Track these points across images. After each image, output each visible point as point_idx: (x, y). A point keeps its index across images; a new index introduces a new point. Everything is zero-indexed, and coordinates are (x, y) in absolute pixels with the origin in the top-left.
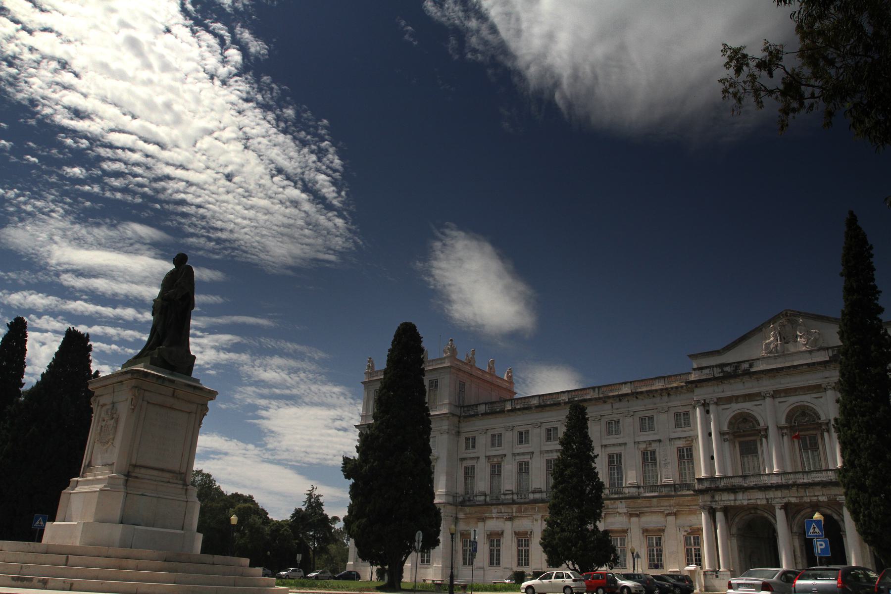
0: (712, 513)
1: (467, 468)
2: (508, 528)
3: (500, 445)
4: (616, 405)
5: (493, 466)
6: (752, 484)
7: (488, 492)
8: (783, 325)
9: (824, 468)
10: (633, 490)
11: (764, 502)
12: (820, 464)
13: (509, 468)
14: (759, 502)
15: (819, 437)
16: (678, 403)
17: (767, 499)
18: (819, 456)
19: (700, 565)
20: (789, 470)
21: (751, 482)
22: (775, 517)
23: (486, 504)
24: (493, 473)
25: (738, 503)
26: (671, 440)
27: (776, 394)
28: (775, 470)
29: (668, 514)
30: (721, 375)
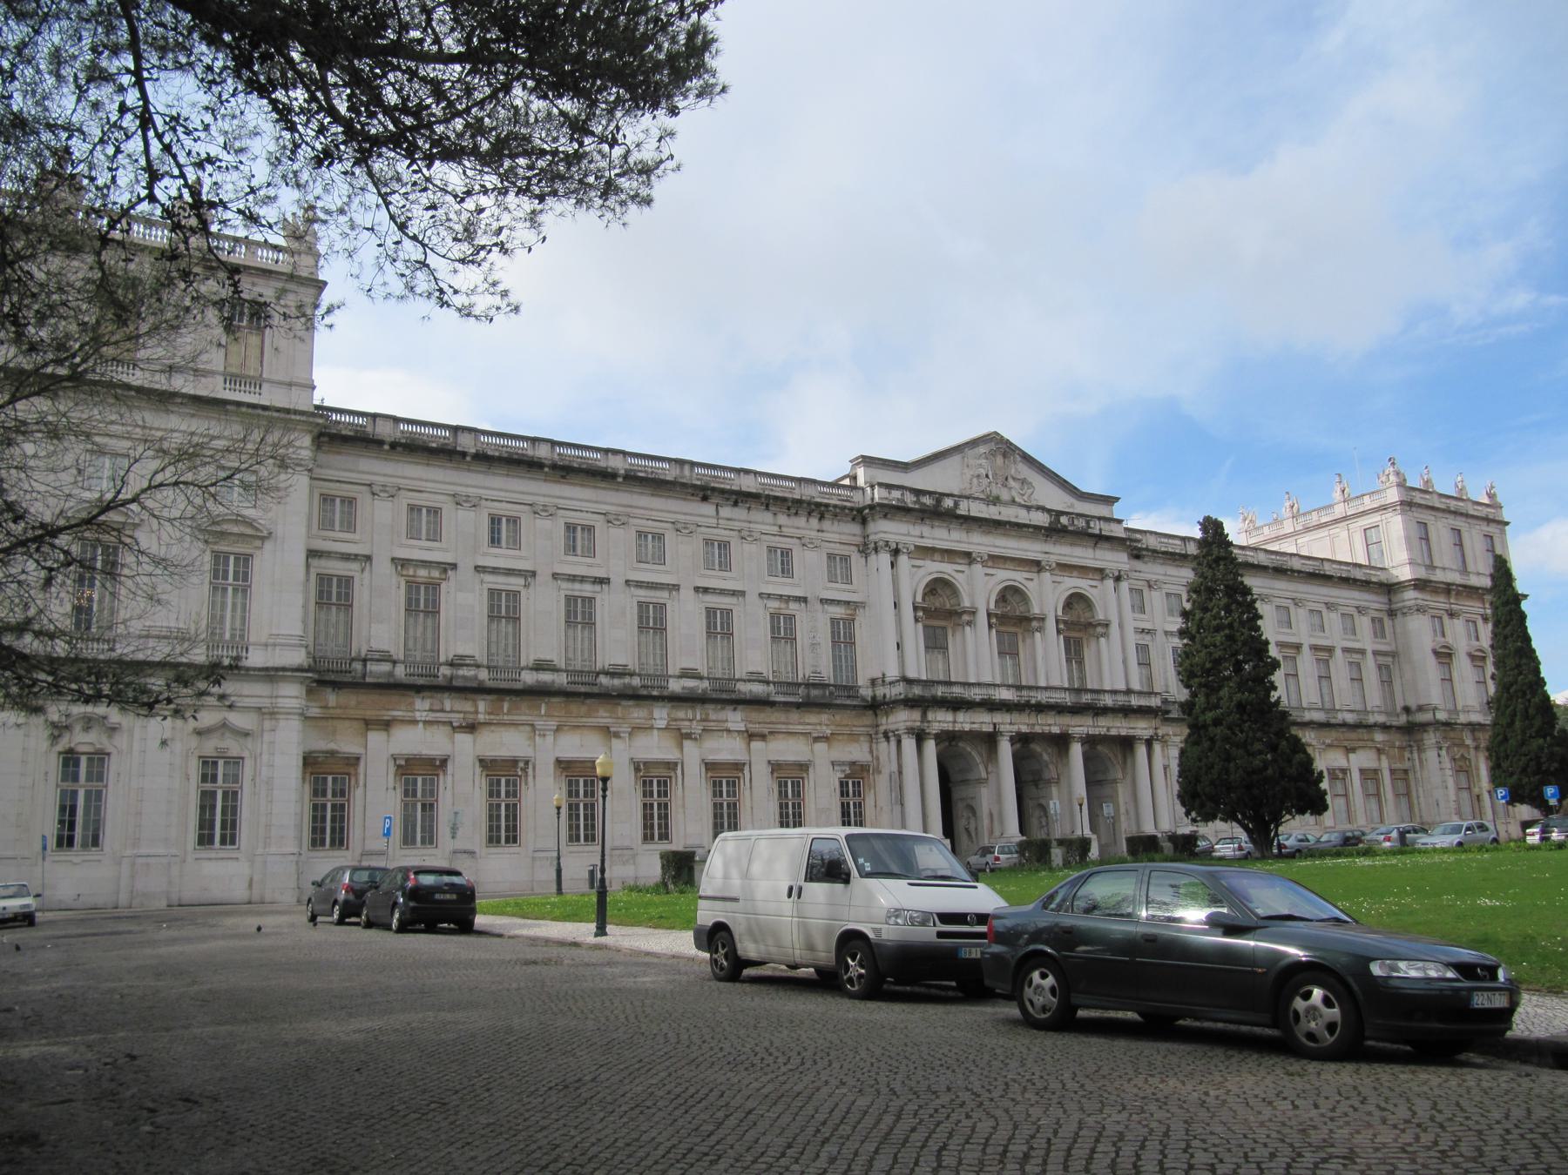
1: (324, 580)
2: (465, 750)
4: (726, 511)
5: (412, 586)
6: (978, 698)
9: (1042, 683)
16: (836, 537)
24: (411, 608)
25: (958, 727)
26: (823, 601)
27: (996, 560)
29: (816, 739)
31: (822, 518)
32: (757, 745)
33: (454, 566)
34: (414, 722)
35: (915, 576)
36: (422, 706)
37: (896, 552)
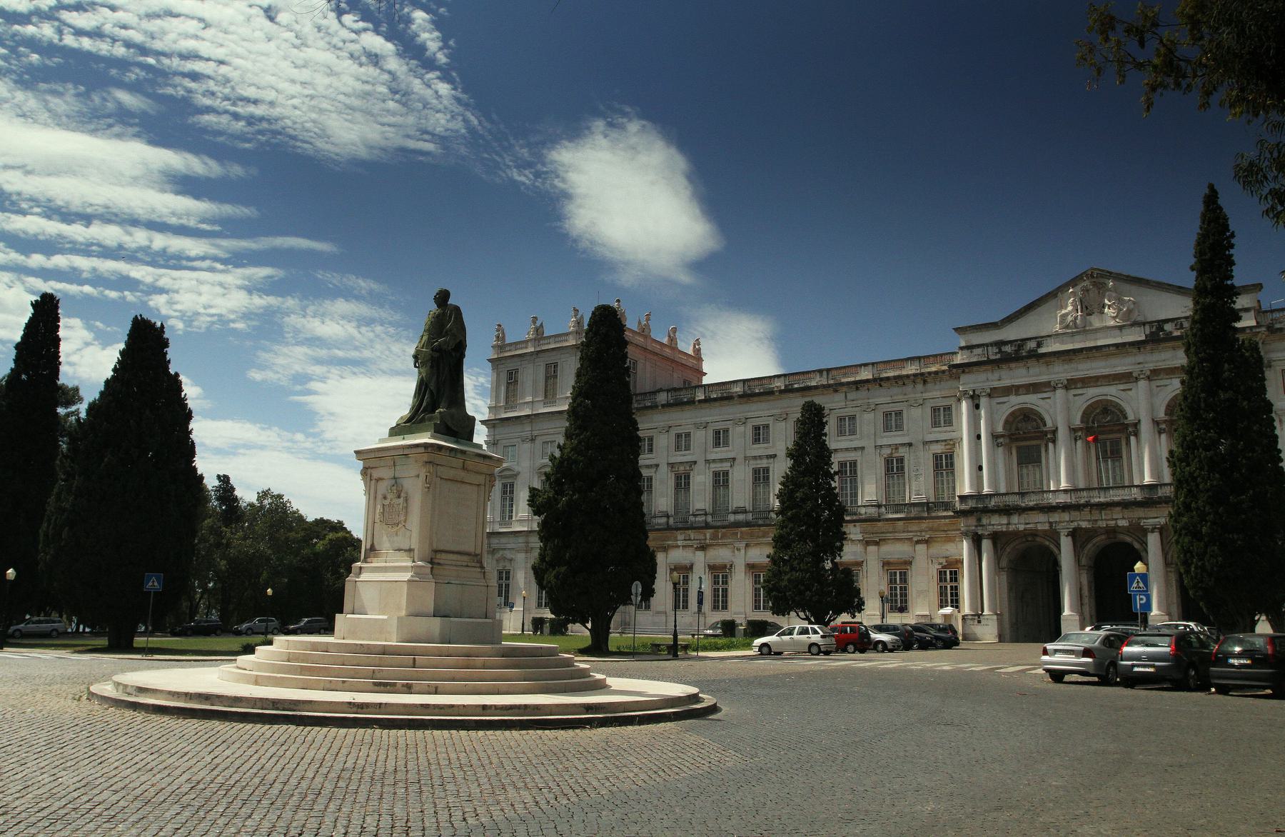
0: (977, 541)
2: (699, 559)
3: (688, 448)
4: (851, 396)
5: (678, 478)
6: (1031, 504)
7: (671, 512)
8: (1085, 290)
10: (872, 511)
11: (1047, 527)
12: (1122, 477)
13: (701, 481)
14: (1040, 527)
15: (1124, 443)
16: (937, 394)
17: (1051, 523)
18: (1121, 467)
20: (1081, 486)
21: (1031, 501)
22: (1058, 546)
23: (668, 528)
24: (678, 486)
25: (1012, 528)
26: (926, 443)
28: (1064, 484)
29: (918, 542)
30: (998, 356)
31: (925, 382)
32: (872, 548)
33: (695, 462)
34: (678, 547)
36: (680, 536)
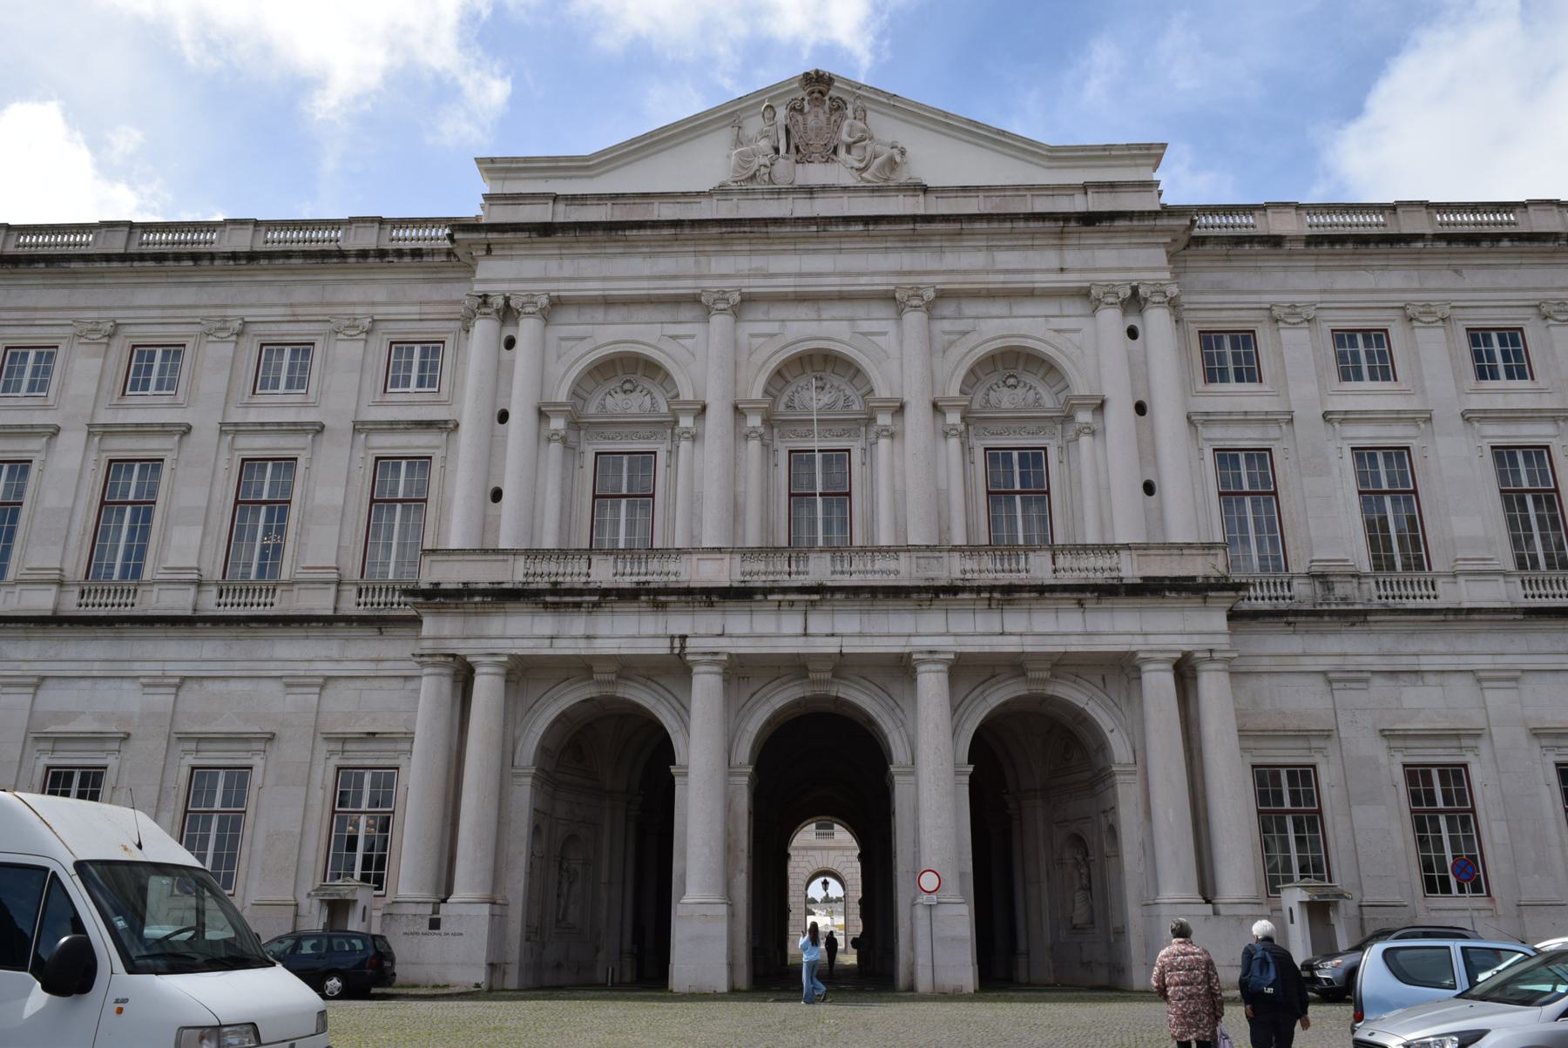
11: (661, 648)
19: (379, 882)
22: (683, 711)
26: (360, 427)
35: (546, 361)
37: (508, 313)
